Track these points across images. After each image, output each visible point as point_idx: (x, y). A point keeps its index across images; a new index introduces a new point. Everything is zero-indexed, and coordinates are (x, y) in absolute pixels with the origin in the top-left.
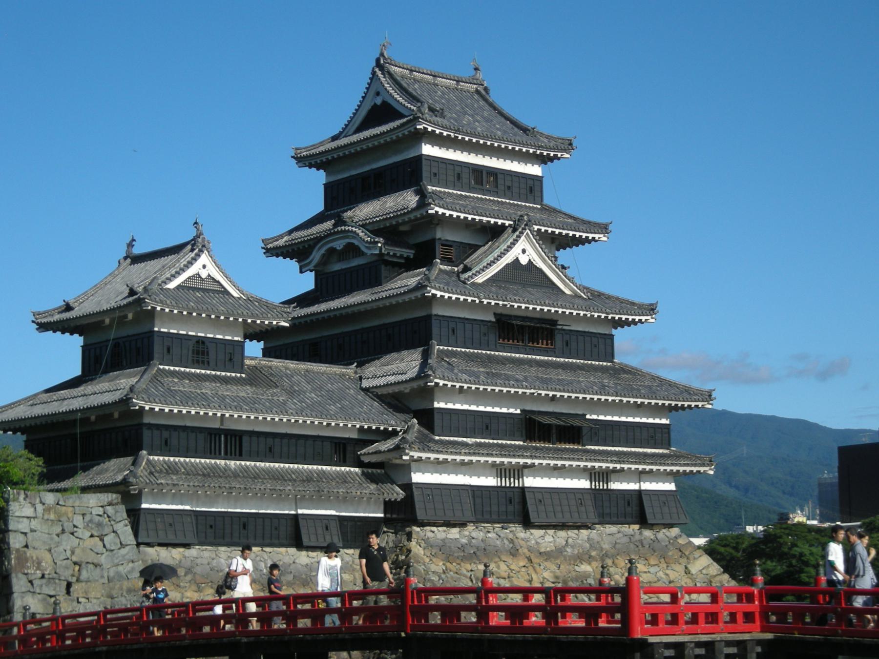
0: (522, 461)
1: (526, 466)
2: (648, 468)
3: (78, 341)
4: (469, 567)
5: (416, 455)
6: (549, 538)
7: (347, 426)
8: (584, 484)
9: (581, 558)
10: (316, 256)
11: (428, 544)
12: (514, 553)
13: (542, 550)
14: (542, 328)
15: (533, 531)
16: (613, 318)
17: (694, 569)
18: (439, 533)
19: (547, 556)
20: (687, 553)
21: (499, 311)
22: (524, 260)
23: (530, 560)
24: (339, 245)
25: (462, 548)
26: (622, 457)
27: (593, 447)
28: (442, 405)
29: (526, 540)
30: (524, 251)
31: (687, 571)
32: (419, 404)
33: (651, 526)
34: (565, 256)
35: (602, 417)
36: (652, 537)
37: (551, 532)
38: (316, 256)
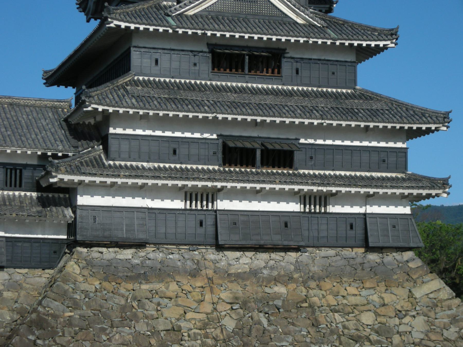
2: (372, 191)
7: (23, 152)
9: (277, 280)
13: (232, 271)
14: (261, 56)
15: (226, 253)
16: (351, 45)
17: (418, 293)
19: (239, 277)
20: (414, 277)
21: (214, 42)
27: (306, 172)
28: (119, 131)
29: (215, 262)
31: (411, 294)
33: (379, 249)
35: (320, 142)
36: (378, 261)
37: (250, 254)
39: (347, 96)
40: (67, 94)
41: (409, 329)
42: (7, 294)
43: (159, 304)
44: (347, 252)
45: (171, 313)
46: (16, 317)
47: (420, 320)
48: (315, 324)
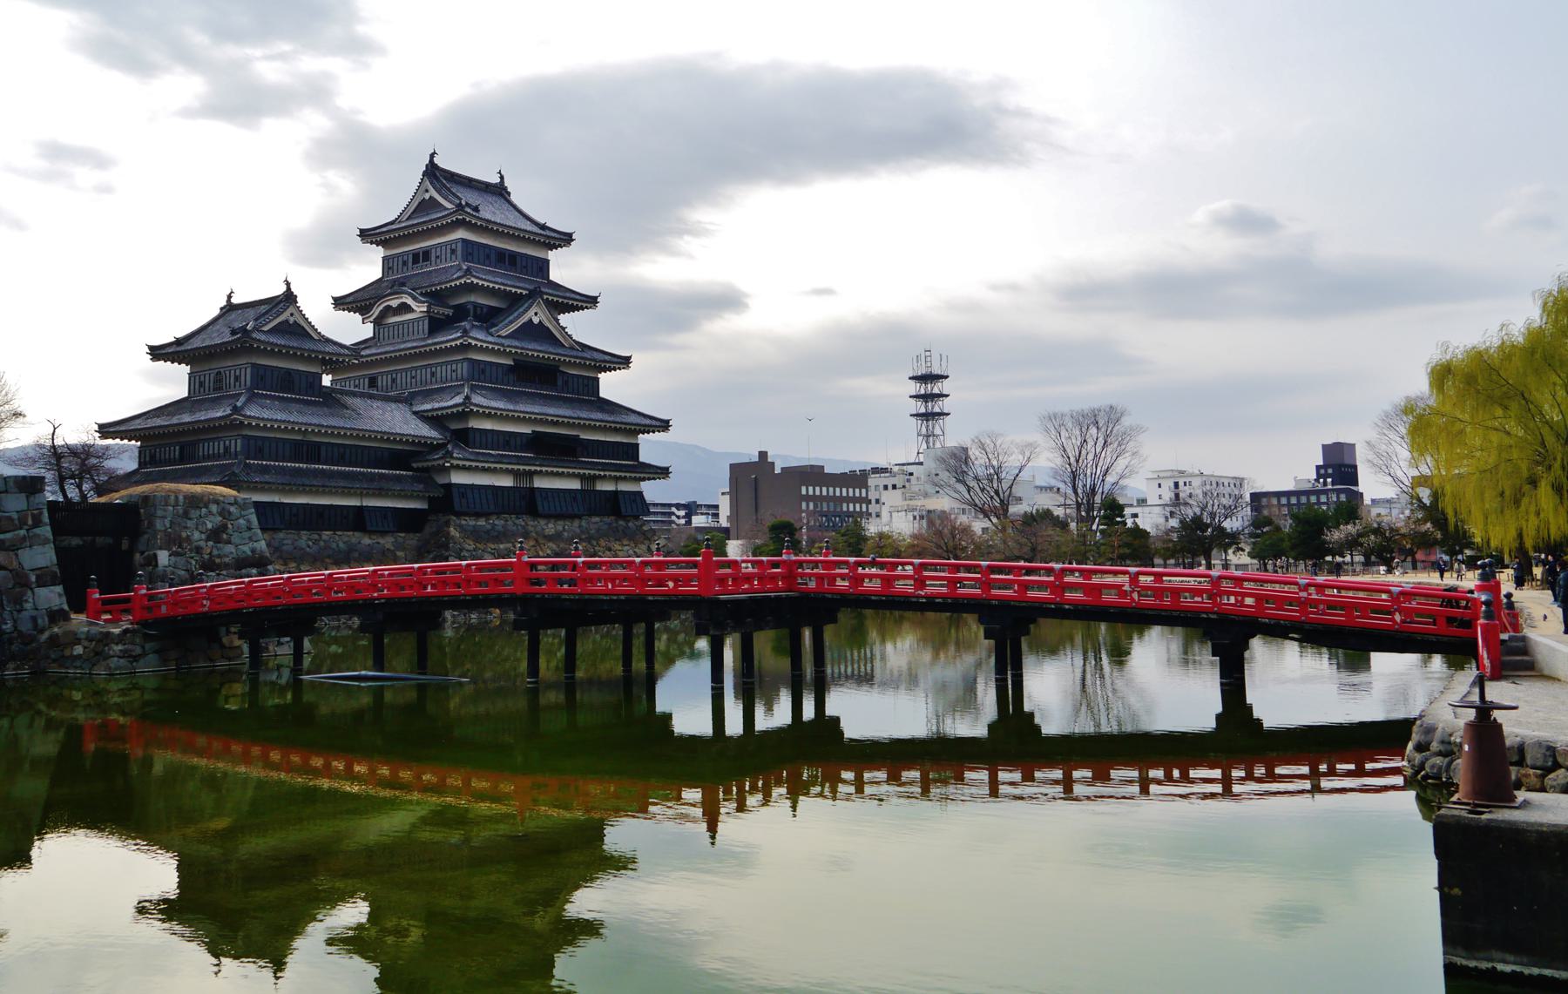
1: (536, 472)
3: (184, 370)
5: (455, 462)
8: (575, 485)
10: (376, 311)
11: (462, 529)
12: (526, 535)
19: (550, 538)
22: (536, 320)
24: (394, 303)
25: (488, 532)
26: (605, 467)
32: (455, 426)
33: (624, 518)
34: (565, 319)
38: (376, 311)
44: (607, 519)
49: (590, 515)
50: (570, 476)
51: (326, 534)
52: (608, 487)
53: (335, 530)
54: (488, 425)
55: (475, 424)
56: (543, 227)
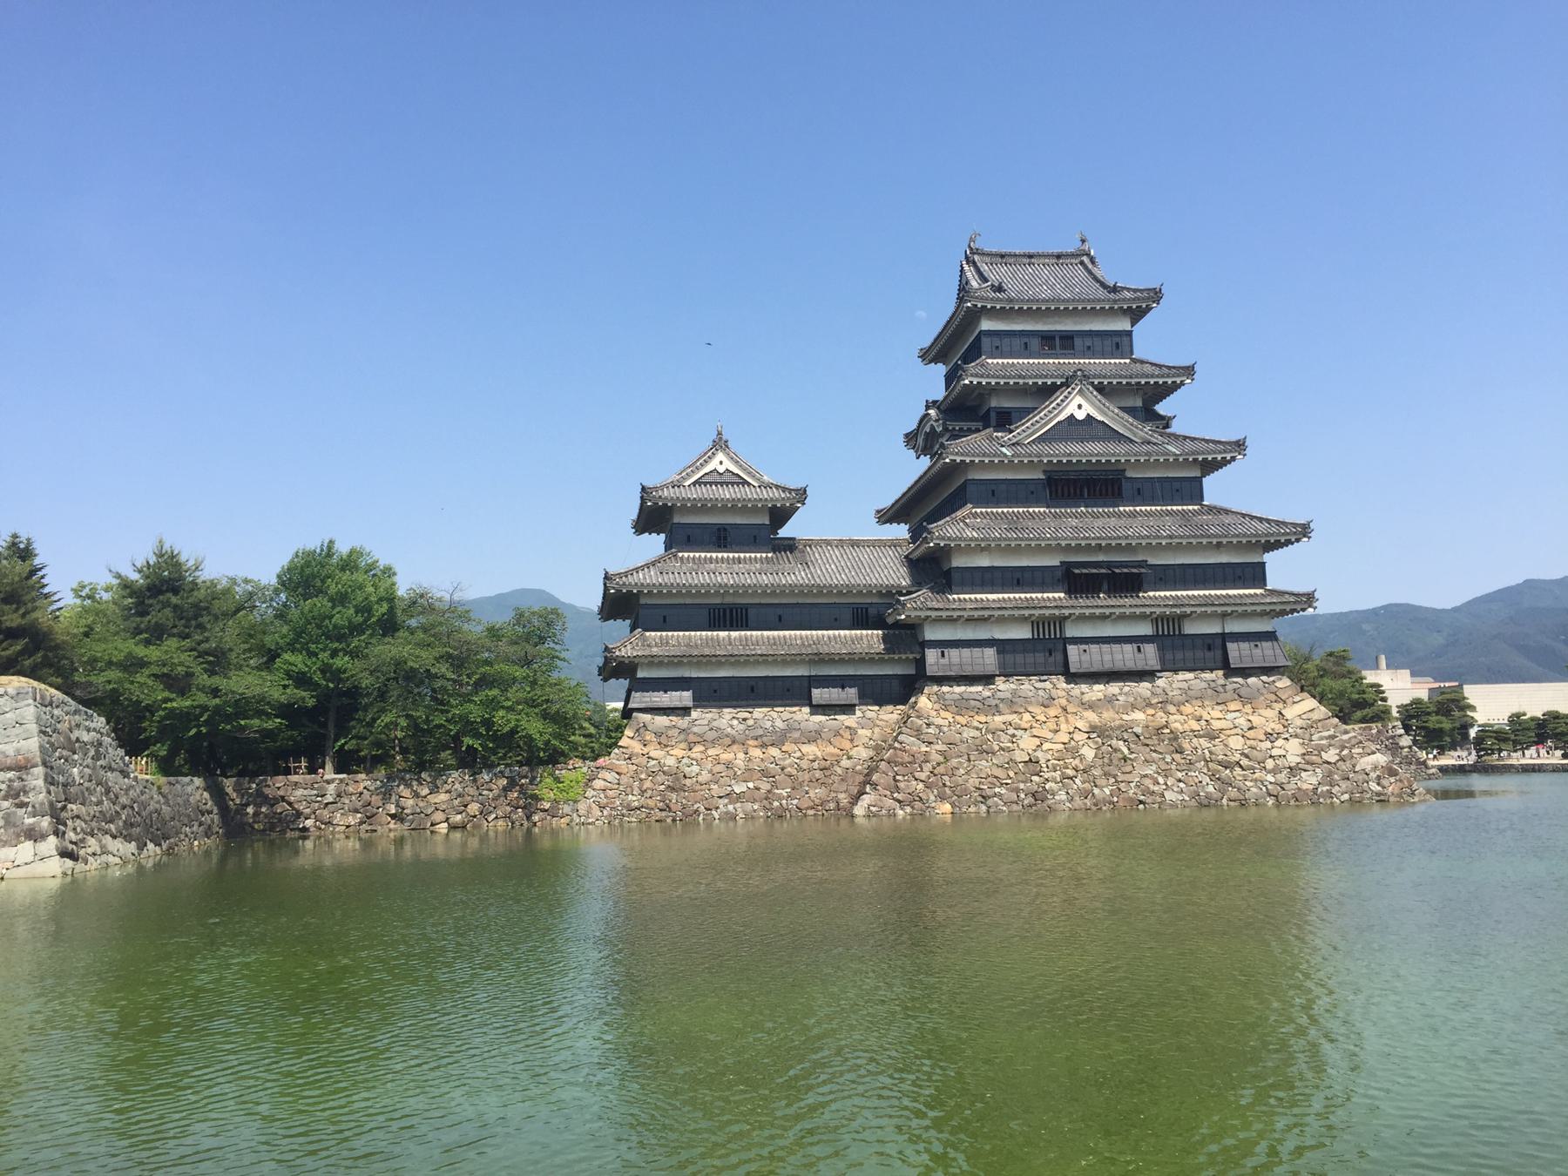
0: (1047, 612)
4: (983, 719)
6: (1097, 687)
8: (1145, 629)
9: (1134, 707)
11: (940, 698)
13: (1086, 698)
17: (1290, 713)
18: (958, 689)
19: (1091, 706)
22: (1080, 415)
23: (1065, 710)
24: (927, 429)
25: (983, 701)
30: (1080, 407)
38: (920, 440)
39: (1195, 513)
40: (901, 531)
41: (1282, 752)
42: (860, 732)
43: (1014, 736)
44: (1208, 676)
45: (1027, 743)
46: (872, 753)
47: (1295, 742)
48: (1180, 751)
49: (1176, 671)
50: (1133, 618)
51: (759, 712)
52: (1213, 628)
53: (773, 706)
54: (984, 561)
55: (958, 562)
56: (1115, 289)
